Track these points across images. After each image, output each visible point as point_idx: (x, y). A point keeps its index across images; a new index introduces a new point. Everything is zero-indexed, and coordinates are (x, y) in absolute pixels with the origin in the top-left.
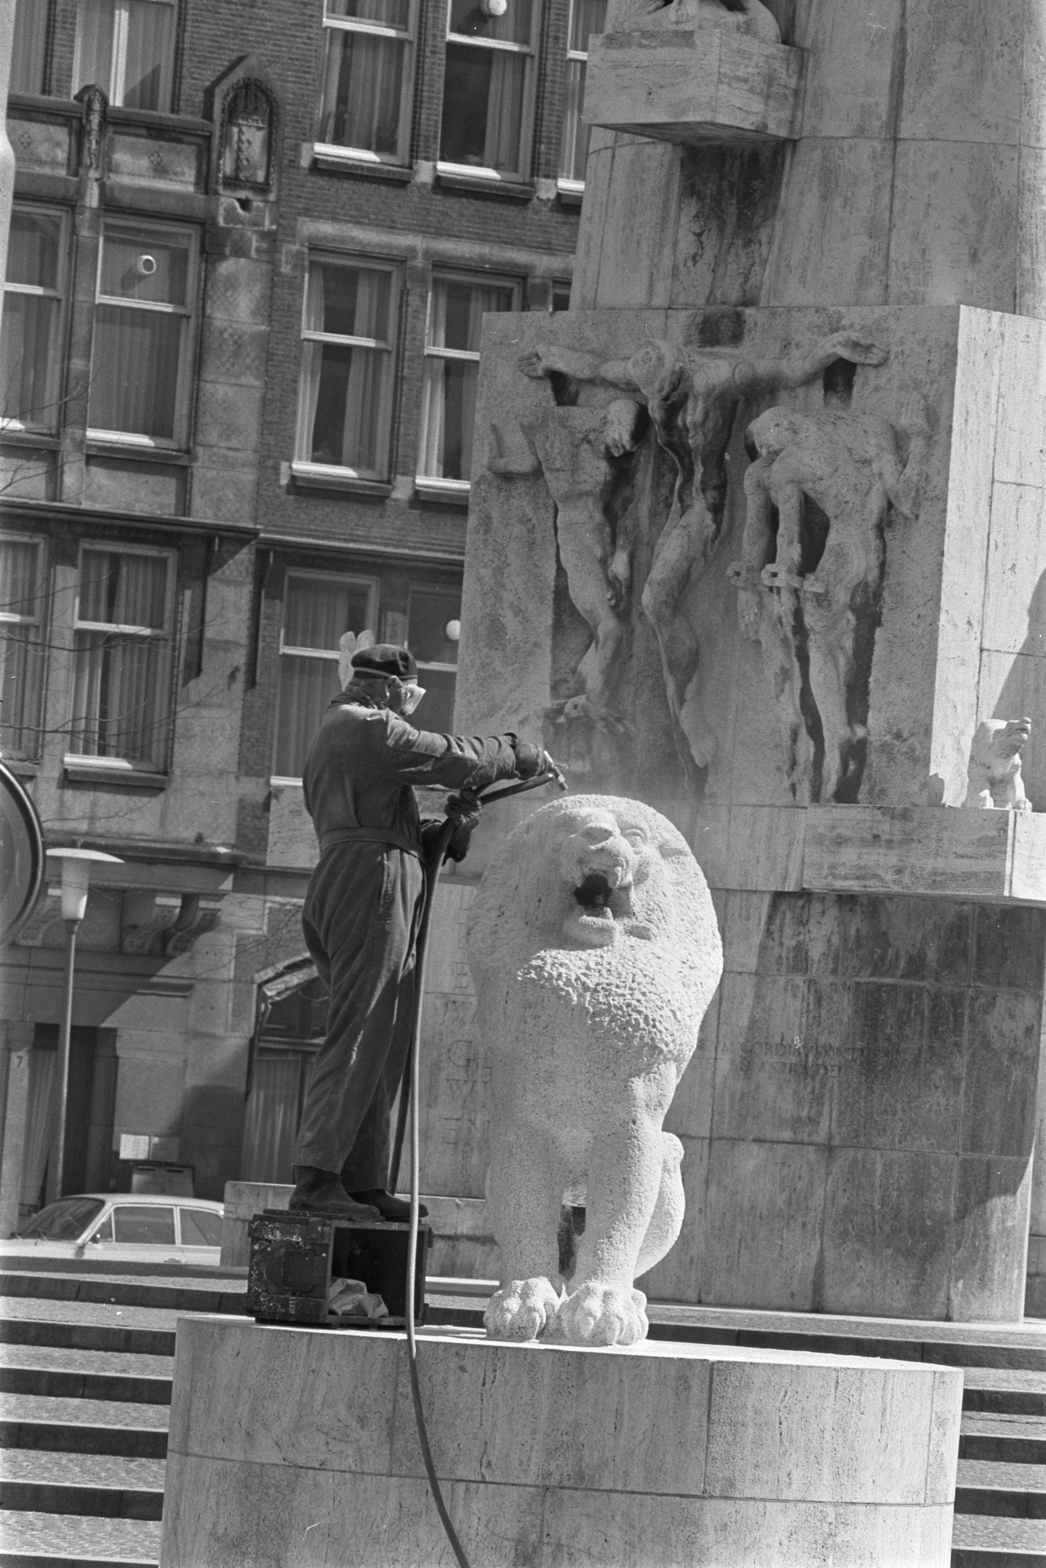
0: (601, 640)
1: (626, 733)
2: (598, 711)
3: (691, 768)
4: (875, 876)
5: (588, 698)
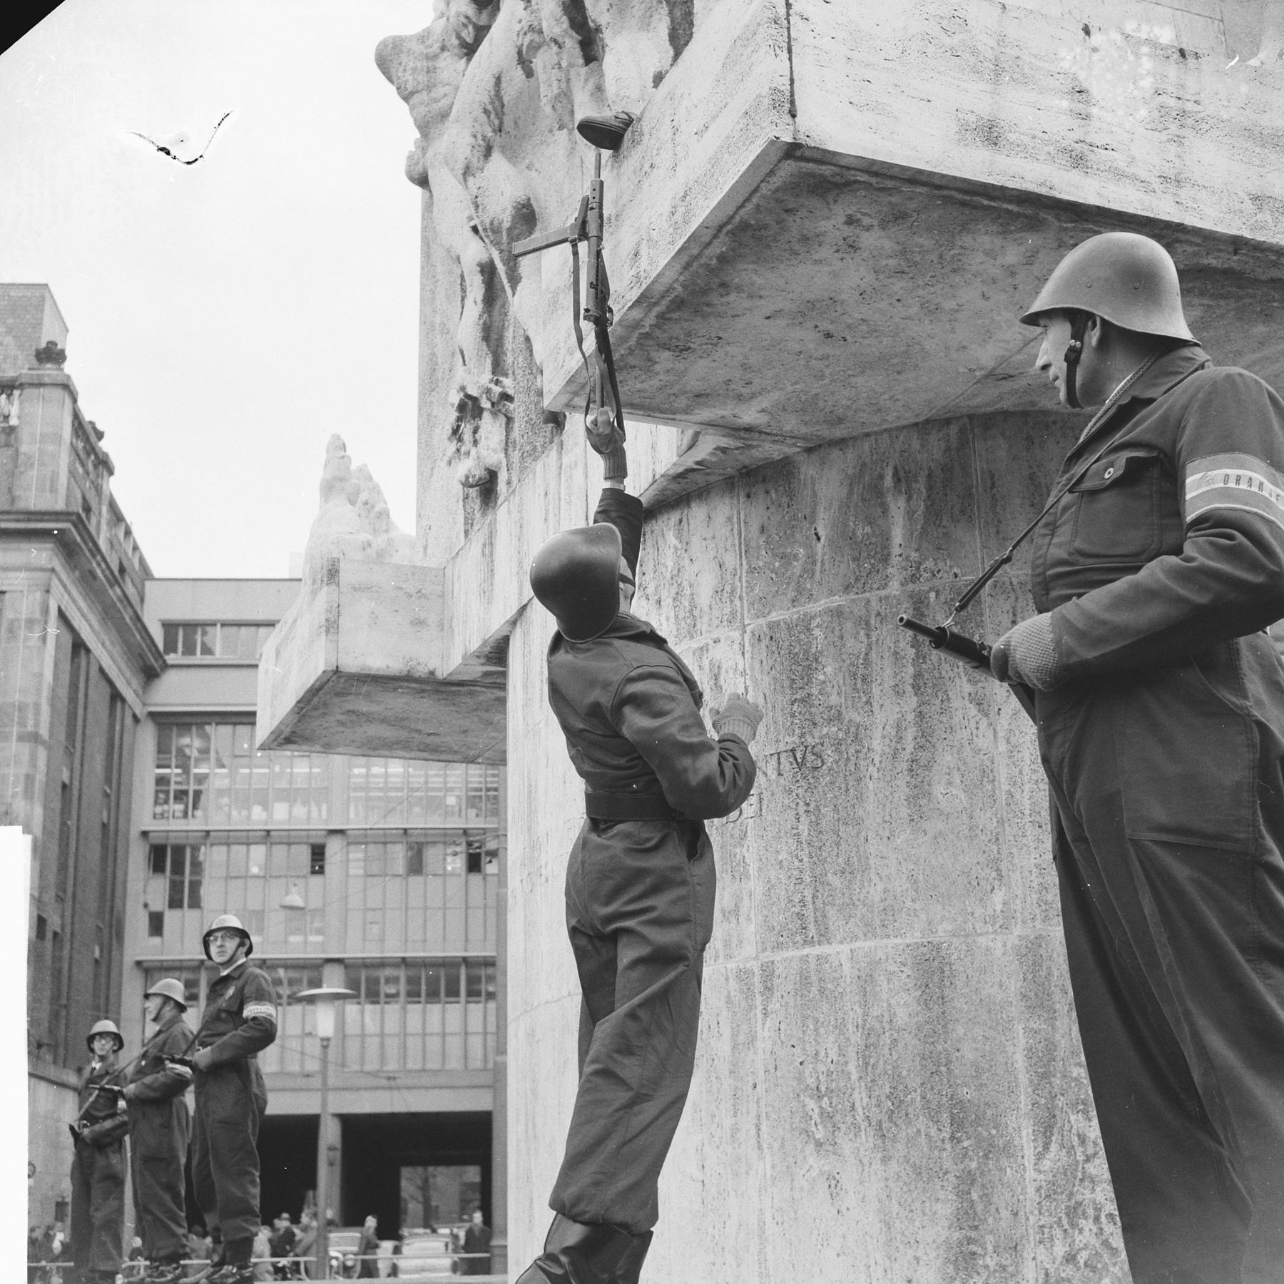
1: (506, 397)
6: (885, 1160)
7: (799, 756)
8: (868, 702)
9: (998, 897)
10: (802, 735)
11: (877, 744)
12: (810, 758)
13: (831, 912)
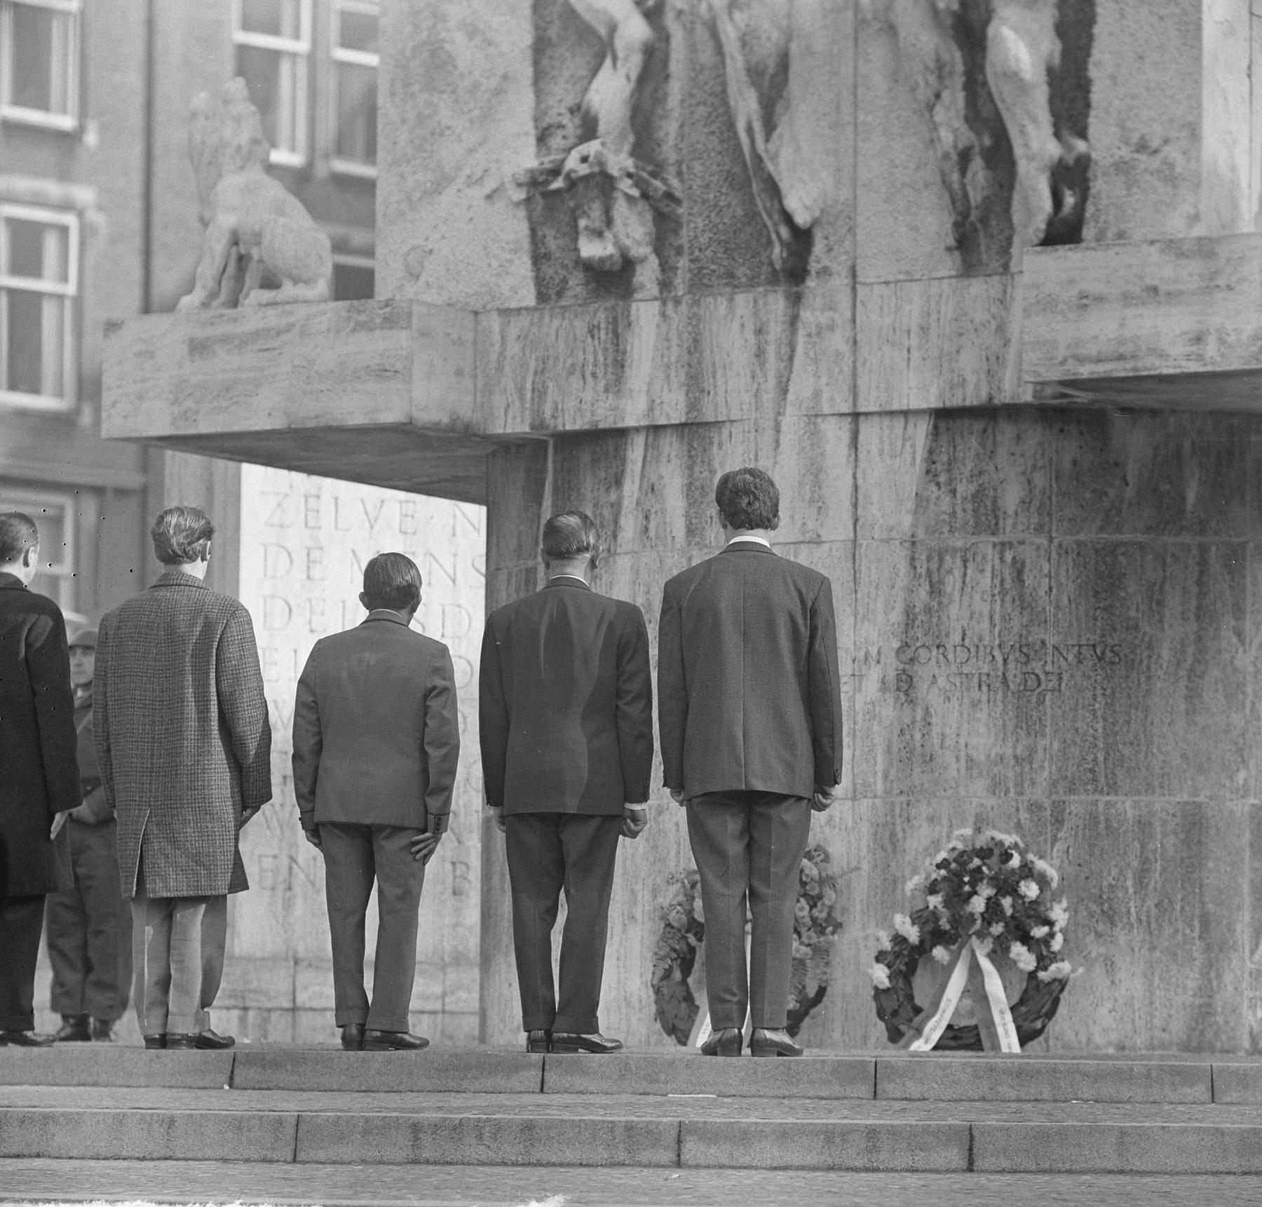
0: (620, 55)
1: (669, 196)
2: (619, 161)
3: (785, 232)
4: (1153, 351)
5: (603, 144)
6: (1152, 948)
7: (1098, 651)
8: (1161, 621)
9: (1242, 775)
10: (1103, 636)
11: (1165, 654)
12: (1108, 654)
13: (1120, 774)
